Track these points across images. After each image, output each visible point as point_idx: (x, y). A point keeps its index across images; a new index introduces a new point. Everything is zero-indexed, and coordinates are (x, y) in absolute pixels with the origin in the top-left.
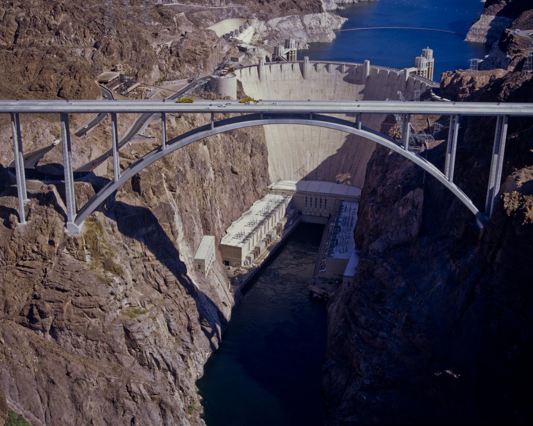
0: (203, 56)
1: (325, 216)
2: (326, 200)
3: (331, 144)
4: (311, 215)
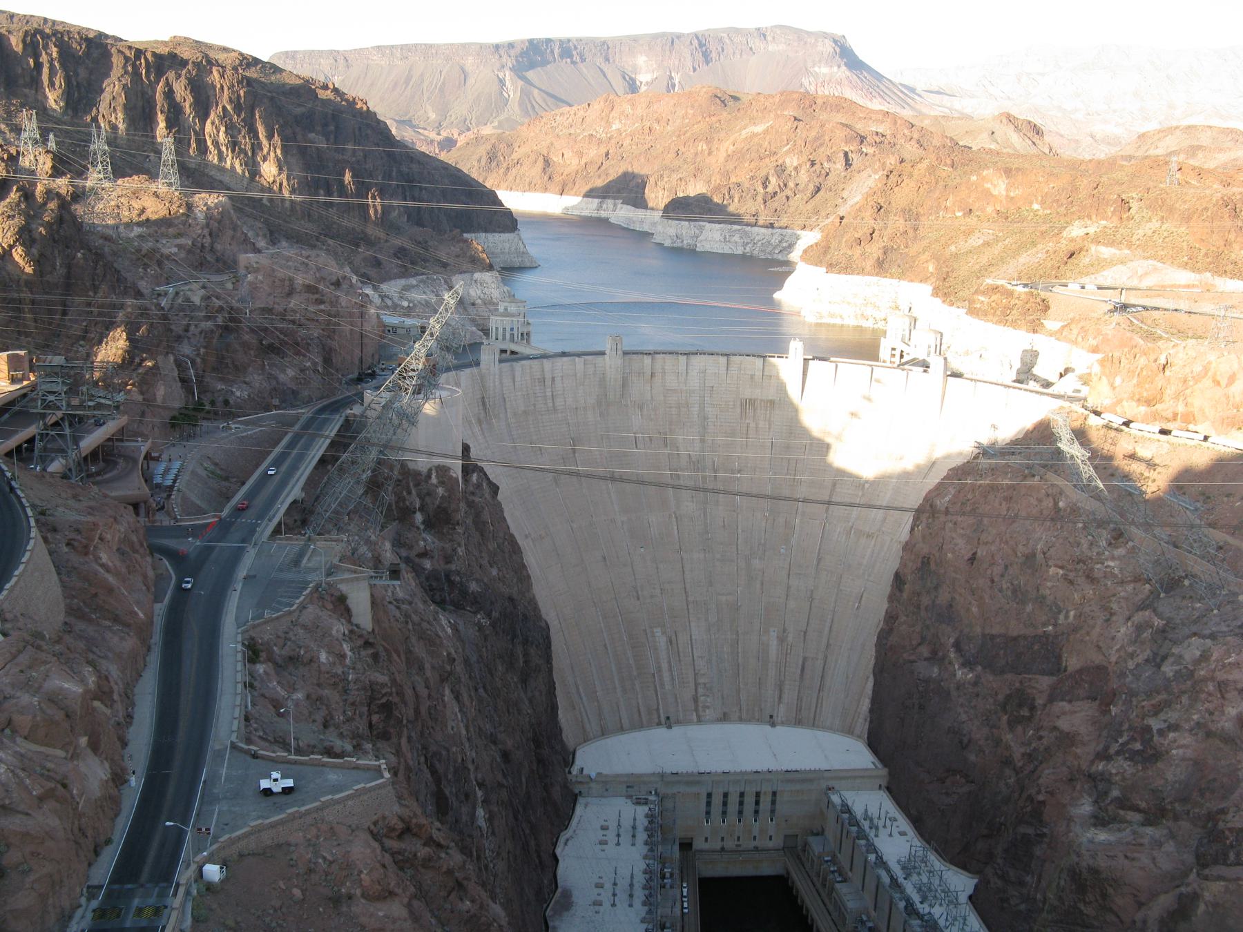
1: (771, 844)
2: (774, 794)
3: (724, 598)
4: (723, 849)
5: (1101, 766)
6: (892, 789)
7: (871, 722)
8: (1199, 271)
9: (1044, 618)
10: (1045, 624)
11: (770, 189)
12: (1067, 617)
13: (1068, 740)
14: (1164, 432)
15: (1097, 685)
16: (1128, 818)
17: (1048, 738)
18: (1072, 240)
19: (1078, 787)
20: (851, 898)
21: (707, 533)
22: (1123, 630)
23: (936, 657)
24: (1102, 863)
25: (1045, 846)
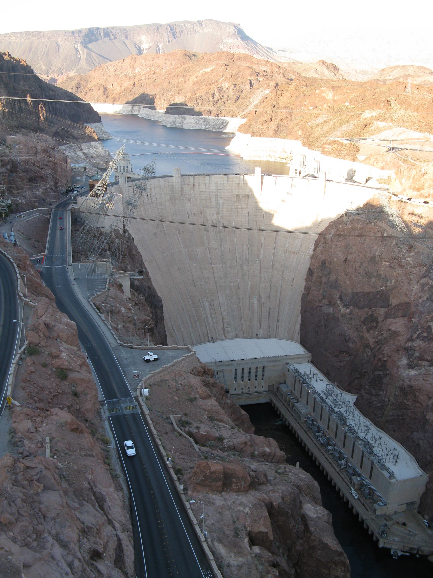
0: (49, 171)
1: (263, 389)
2: (264, 367)
3: (232, 284)
4: (242, 393)
5: (410, 344)
6: (315, 362)
7: (301, 334)
8: (423, 132)
9: (381, 284)
10: (381, 287)
11: (216, 98)
12: (391, 283)
13: (395, 334)
14: (425, 202)
15: (406, 310)
16: (423, 364)
17: (385, 334)
18: (366, 119)
19: (401, 353)
20: (303, 408)
21: (223, 255)
22: (416, 287)
23: (331, 304)
24: (414, 383)
25: (388, 379)
